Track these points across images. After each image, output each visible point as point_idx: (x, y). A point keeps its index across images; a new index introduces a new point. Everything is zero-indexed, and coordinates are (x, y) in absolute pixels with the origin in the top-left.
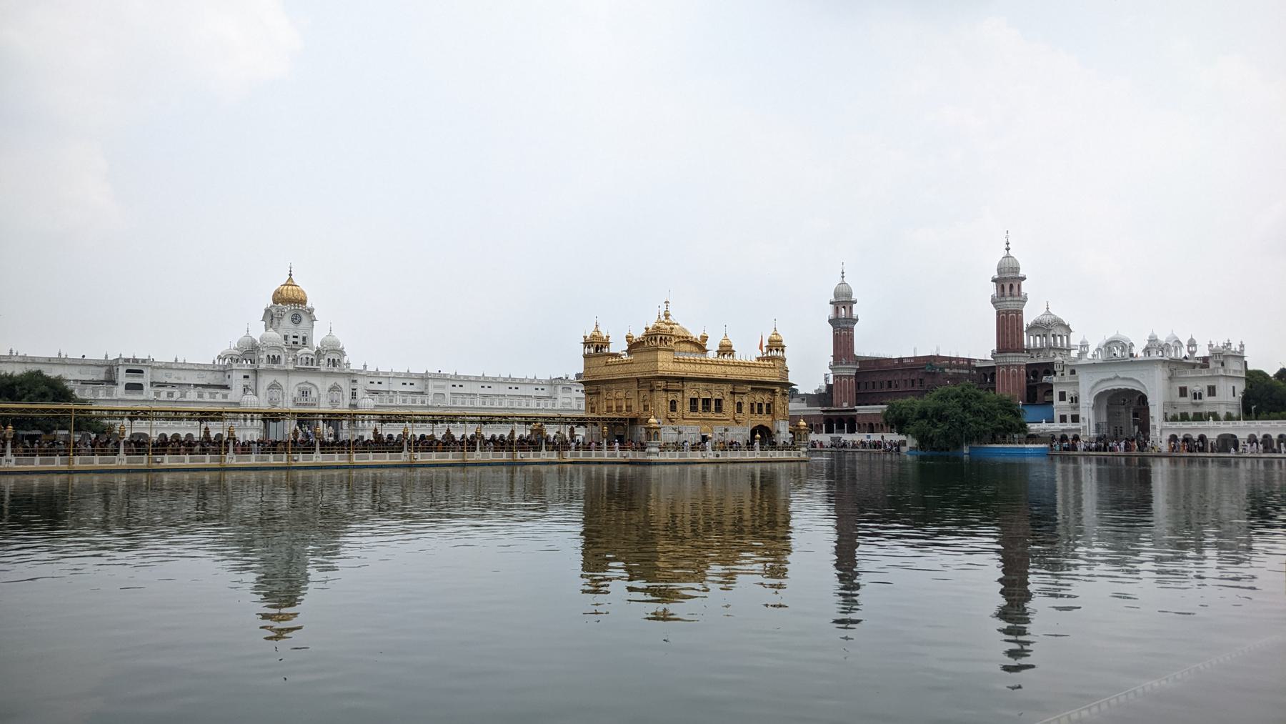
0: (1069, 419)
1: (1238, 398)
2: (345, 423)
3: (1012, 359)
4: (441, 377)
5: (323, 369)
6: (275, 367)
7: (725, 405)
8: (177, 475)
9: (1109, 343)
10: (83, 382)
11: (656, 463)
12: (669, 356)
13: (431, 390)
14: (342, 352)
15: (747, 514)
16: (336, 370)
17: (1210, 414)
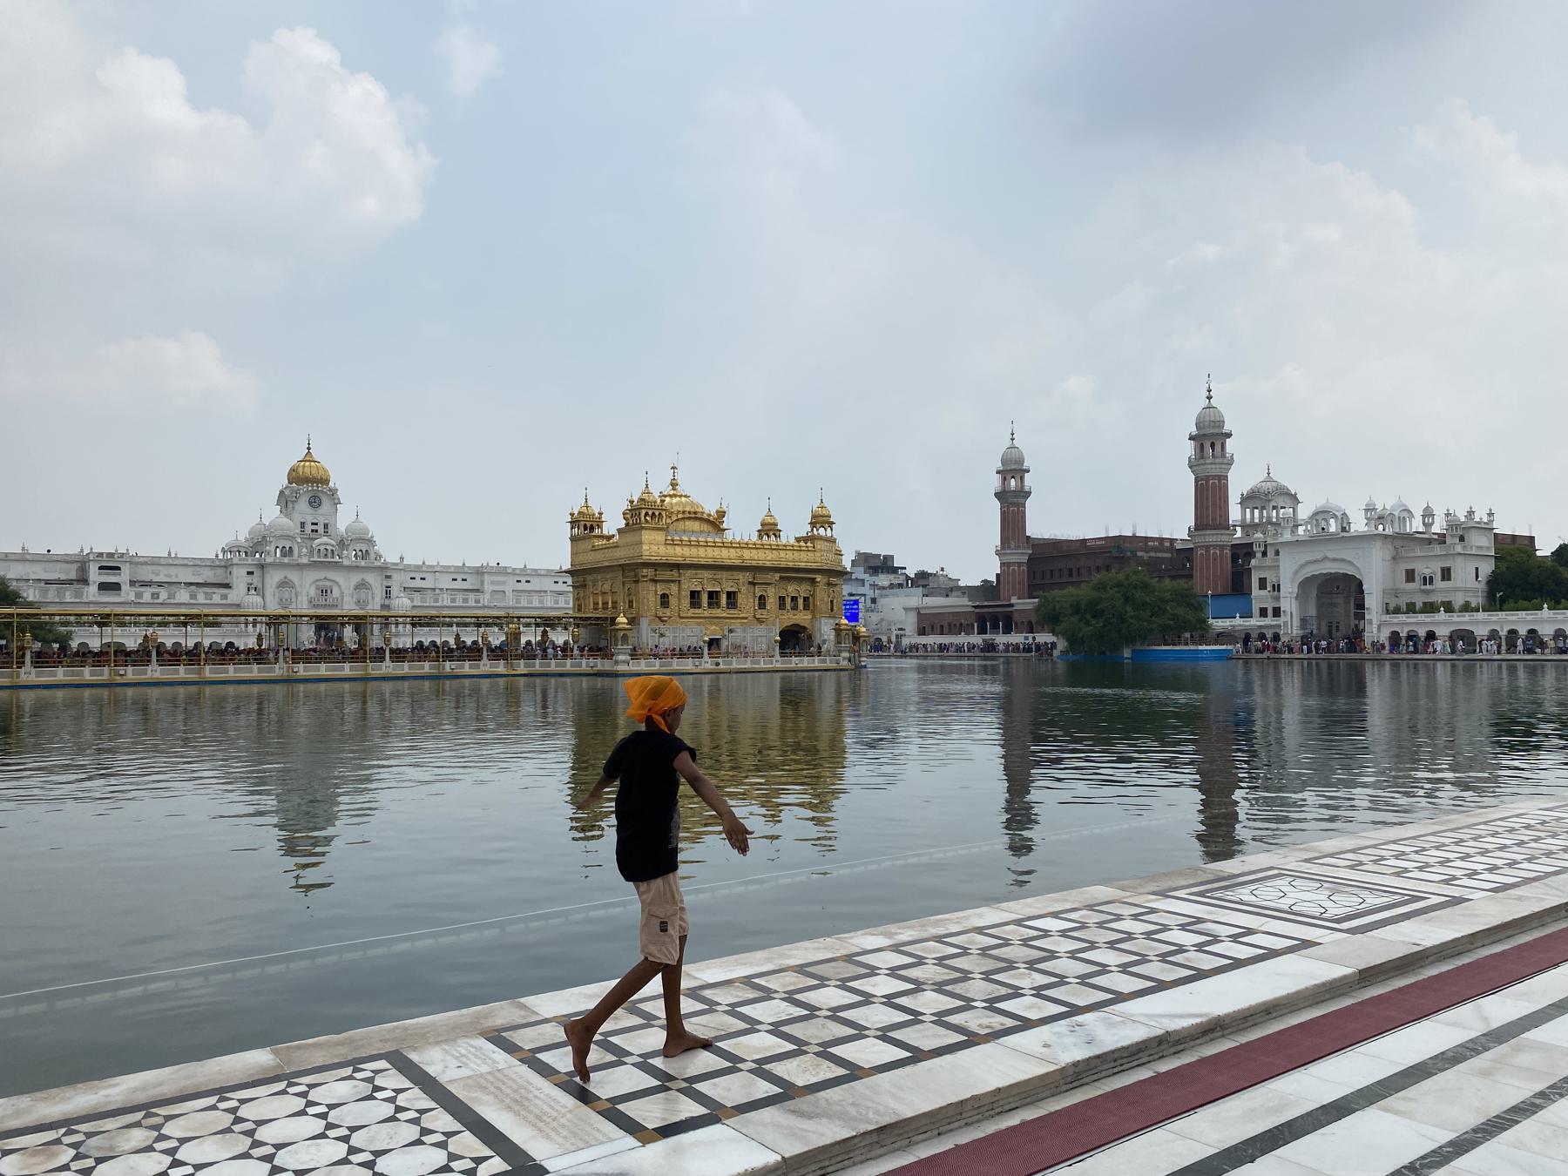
0: (1270, 612)
1: (1481, 586)
2: (376, 628)
3: (1212, 537)
4: (501, 571)
5: (346, 562)
6: (286, 560)
7: (741, 599)
8: (77, 692)
9: (1316, 514)
10: (48, 582)
11: (624, 675)
12: (660, 537)
13: (488, 588)
14: (371, 542)
15: (773, 736)
16: (363, 563)
17: (1443, 603)
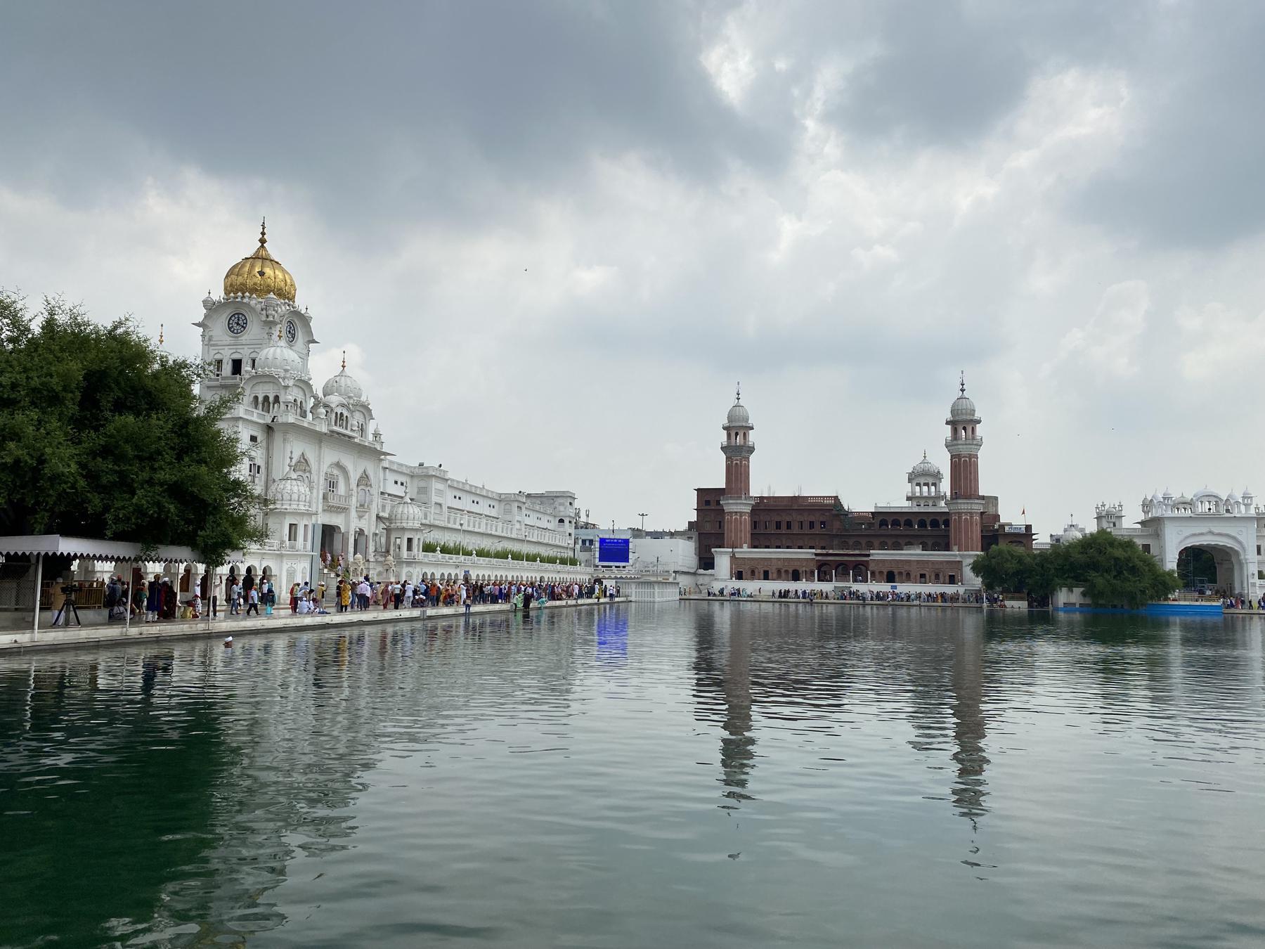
3: (963, 506)
14: (366, 410)
